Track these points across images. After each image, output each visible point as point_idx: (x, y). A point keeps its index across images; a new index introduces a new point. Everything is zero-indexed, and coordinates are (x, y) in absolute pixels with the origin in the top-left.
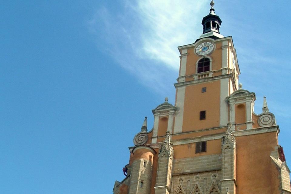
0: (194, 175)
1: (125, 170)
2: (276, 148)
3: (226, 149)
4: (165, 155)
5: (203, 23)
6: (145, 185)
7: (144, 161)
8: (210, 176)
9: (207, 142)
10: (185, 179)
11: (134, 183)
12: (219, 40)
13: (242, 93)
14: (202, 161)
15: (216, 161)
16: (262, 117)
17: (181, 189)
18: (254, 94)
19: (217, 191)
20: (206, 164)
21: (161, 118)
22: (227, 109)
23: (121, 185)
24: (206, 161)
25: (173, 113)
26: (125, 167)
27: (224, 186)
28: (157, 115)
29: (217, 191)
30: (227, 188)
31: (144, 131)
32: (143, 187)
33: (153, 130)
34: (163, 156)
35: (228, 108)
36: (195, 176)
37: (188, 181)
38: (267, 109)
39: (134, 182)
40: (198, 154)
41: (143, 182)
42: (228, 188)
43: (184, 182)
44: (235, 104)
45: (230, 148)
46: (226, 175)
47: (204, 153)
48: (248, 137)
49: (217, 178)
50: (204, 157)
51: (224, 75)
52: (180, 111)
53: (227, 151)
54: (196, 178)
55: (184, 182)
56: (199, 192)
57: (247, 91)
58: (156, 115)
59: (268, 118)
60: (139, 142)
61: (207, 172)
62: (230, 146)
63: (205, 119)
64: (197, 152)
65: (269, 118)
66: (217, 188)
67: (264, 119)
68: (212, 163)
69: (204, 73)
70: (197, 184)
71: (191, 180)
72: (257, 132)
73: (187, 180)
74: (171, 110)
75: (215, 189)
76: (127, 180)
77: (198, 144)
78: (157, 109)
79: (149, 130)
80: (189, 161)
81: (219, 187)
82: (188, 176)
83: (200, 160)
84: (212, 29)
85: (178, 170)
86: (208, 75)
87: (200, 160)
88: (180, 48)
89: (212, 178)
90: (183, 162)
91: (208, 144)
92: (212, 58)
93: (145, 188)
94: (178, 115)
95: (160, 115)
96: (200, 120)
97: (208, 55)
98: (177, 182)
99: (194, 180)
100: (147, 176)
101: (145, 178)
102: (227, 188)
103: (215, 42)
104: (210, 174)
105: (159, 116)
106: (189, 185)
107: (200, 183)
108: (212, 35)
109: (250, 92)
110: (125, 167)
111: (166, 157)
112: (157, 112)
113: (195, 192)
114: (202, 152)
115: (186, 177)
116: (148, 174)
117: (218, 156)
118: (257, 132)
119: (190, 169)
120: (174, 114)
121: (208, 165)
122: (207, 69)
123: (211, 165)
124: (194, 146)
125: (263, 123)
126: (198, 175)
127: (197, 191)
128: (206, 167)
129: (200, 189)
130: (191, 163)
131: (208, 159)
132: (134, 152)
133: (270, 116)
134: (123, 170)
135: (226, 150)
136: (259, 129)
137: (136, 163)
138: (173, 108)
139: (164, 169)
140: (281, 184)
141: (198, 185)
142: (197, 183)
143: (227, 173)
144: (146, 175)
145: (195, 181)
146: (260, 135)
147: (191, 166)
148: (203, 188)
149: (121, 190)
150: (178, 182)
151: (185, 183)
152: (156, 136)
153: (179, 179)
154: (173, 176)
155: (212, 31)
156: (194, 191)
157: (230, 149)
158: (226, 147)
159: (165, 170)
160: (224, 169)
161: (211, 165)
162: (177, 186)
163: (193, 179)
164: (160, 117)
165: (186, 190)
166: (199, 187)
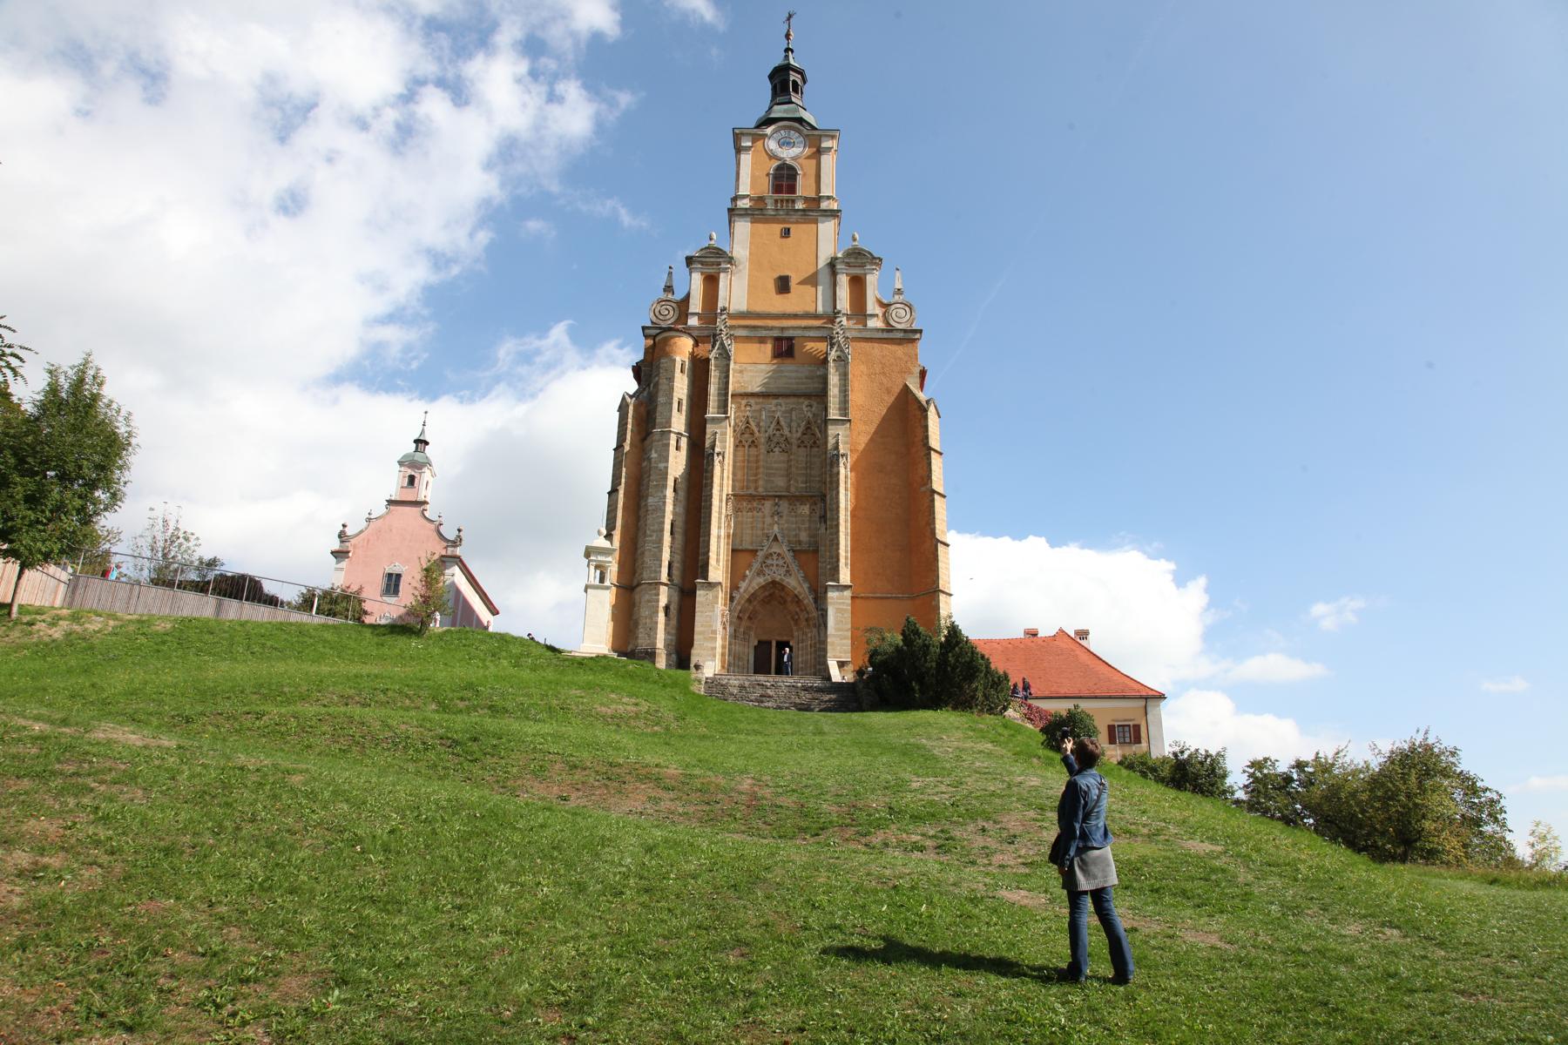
1: (638, 371)
2: (917, 371)
5: (771, 77)
10: (756, 403)
12: (816, 133)
13: (859, 253)
15: (812, 378)
16: (893, 307)
18: (881, 260)
24: (794, 375)
31: (670, 296)
33: (688, 296)
36: (775, 401)
47: (789, 361)
51: (825, 211)
52: (740, 267)
54: (776, 405)
57: (870, 253)
60: (661, 317)
61: (795, 395)
69: (785, 196)
73: (758, 407)
77: (778, 339)
79: (679, 296)
82: (761, 400)
84: (794, 99)
86: (793, 201)
88: (737, 131)
89: (805, 409)
92: (802, 169)
97: (794, 159)
103: (807, 135)
104: (801, 400)
108: (797, 115)
109: (876, 255)
118: (885, 335)
121: (797, 383)
122: (792, 189)
123: (803, 383)
125: (896, 319)
126: (780, 401)
128: (795, 386)
131: (797, 371)
132: (657, 340)
133: (907, 309)
136: (888, 331)
140: (927, 437)
141: (781, 419)
142: (779, 414)
148: (790, 426)
150: (743, 408)
154: (732, 395)
155: (793, 103)
161: (803, 383)
165: (758, 425)
166: (782, 423)
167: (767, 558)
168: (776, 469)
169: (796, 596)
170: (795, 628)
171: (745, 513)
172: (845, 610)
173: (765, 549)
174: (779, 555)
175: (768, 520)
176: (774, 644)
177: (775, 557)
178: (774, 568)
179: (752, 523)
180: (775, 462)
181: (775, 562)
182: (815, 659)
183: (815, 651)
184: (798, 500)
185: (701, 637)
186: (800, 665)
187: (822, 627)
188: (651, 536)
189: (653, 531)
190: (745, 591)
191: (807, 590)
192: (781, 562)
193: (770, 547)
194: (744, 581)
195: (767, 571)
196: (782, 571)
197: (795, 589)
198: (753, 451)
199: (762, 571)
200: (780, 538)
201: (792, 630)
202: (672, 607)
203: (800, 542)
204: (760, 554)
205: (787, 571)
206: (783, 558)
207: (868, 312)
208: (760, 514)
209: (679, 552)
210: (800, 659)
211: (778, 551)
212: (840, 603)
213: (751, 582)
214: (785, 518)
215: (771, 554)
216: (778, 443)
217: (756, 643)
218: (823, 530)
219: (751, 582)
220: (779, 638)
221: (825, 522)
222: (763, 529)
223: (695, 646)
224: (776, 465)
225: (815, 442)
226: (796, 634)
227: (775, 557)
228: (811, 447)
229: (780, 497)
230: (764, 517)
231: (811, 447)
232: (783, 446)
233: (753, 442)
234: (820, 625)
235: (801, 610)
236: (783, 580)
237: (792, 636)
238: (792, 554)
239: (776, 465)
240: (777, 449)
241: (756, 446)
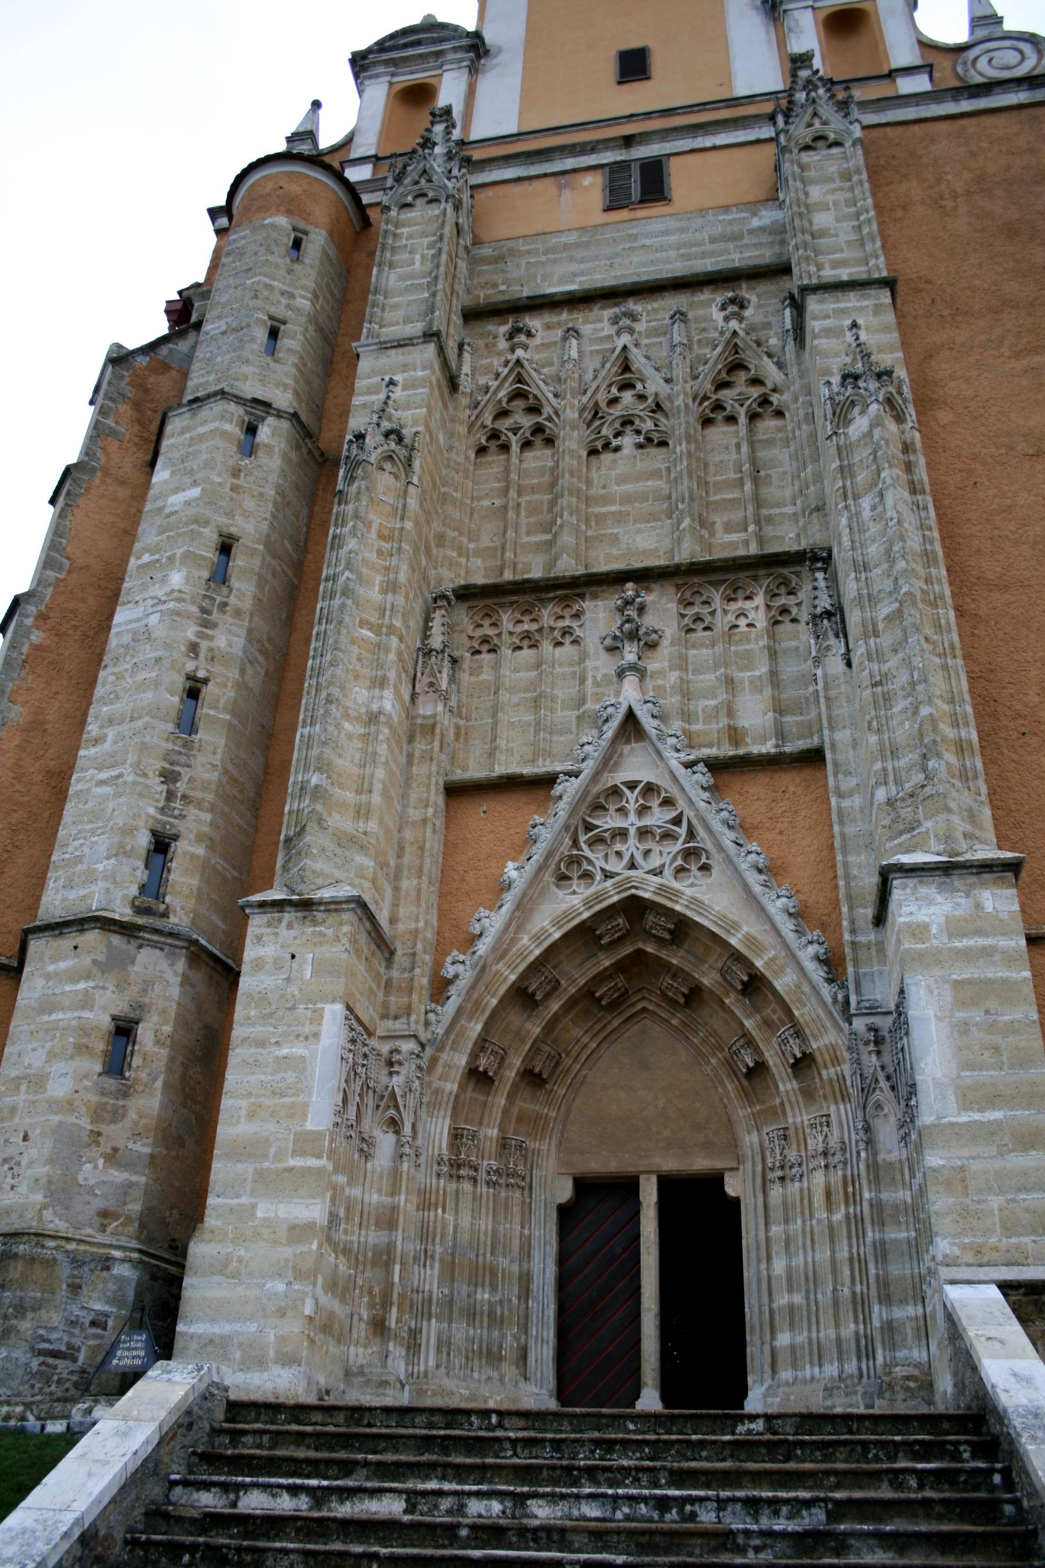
0: (602, 308)
3: (807, 148)
4: (424, 195)
6: (292, 342)
7: (295, 229)
8: (706, 304)
9: (674, 162)
10: (548, 327)
11: (224, 333)
14: (648, 242)
17: (520, 380)
19: (756, 381)
20: (672, 253)
21: (397, 88)
22: (768, 33)
23: (142, 361)
24: (673, 239)
25: (465, 64)
26: (177, 297)
27: (828, 317)
28: (377, 76)
29: (756, 381)
30: (848, 322)
32: (281, 355)
34: (410, 199)
35: (772, 29)
37: (569, 330)
38: (999, 21)
39: (224, 328)
40: (623, 214)
41: (282, 327)
42: (860, 322)
43: (542, 344)
44: (812, 7)
45: (830, 146)
46: (827, 266)
47: (657, 210)
48: (916, 129)
49: (747, 313)
50: (658, 226)
52: (501, 59)
53: (818, 158)
54: (615, 320)
55: (537, 341)
56: (639, 386)
58: (370, 77)
59: (1016, 53)
62: (832, 136)
63: (649, 78)
64: (616, 201)
65: (1021, 52)
66: (750, 358)
67: (990, 61)
68: (709, 247)
70: (625, 347)
71: (586, 329)
72: (966, 105)
74: (455, 49)
75: (747, 369)
76: (183, 346)
77: (618, 170)
78: (382, 46)
80: (566, 247)
81: (770, 355)
82: (564, 316)
83: (633, 238)
85: (503, 288)
87: (633, 238)
89: (718, 316)
90: (529, 252)
91: (674, 166)
93: (293, 359)
94: (494, 72)
95: (393, 75)
96: (619, 83)
98: (495, 345)
99: (603, 329)
100: (308, 303)
101: (298, 310)
102: (854, 325)
104: (705, 295)
105: (388, 78)
106: (574, 354)
107: (646, 341)
110: (177, 297)
111: (434, 205)
112: (374, 64)
113: (614, 390)
114: (641, 202)
115: (549, 317)
116: (316, 296)
117: (744, 215)
118: (966, 105)
119: (573, 282)
120: (474, 70)
123: (704, 255)
124: (593, 186)
127: (629, 386)
129: (649, 371)
130: (579, 254)
131: (683, 230)
132: (235, 210)
134: (168, 312)
135: (811, 153)
137: (244, 237)
138: (465, 42)
139: (418, 257)
142: (625, 339)
143: (838, 256)
144: (303, 297)
145: (606, 333)
146: (987, 121)
147: (583, 266)
149: (140, 384)
150: (503, 344)
151: (546, 346)
152: (372, 152)
153: (504, 329)
156: (610, 385)
157: (835, 151)
158: (808, 140)
159: (422, 264)
160: (813, 237)
161: (704, 255)
162: (495, 363)
163: (599, 325)
164: (391, 84)
167: (598, 808)
168: (627, 499)
169: (738, 957)
170: (742, 1113)
171: (506, 652)
172: (1003, 990)
173: (588, 768)
174: (650, 789)
175: (602, 665)
176: (649, 1194)
177: (632, 798)
178: (631, 846)
179: (533, 685)
180: (621, 480)
181: (632, 822)
182: (858, 1263)
183: (855, 1223)
184: (716, 584)
185: (246, 1169)
186: (782, 1300)
187: (883, 1093)
188: (97, 741)
189: (111, 722)
190: (500, 951)
191: (787, 926)
192: (658, 817)
193: (608, 762)
194: (495, 905)
195: (596, 857)
196: (666, 854)
197: (735, 926)
198: (538, 458)
199: (574, 861)
200: (649, 724)
201: (730, 1125)
202: (145, 1034)
203: (735, 735)
204: (568, 790)
205: (689, 854)
206: (668, 802)
207: (895, 65)
208: (568, 650)
209: (210, 797)
210: (779, 1266)
211: (645, 776)
212: (968, 955)
213: (523, 909)
214: (666, 648)
215: (615, 792)
216: (627, 422)
217: (565, 1192)
218: (835, 664)
219: (523, 909)
220: (671, 1164)
221: (842, 632)
222: (582, 701)
223: (211, 1220)
224: (628, 487)
225: (765, 401)
226: (750, 1140)
227: (632, 798)
228: (753, 417)
229: (644, 577)
230: (583, 657)
231: (753, 417)
232: (649, 425)
233: (538, 429)
234: (867, 1090)
235: (768, 1024)
236: (676, 894)
237: (733, 1146)
238: (702, 776)
239: (628, 487)
240: (628, 441)
241: (550, 442)
